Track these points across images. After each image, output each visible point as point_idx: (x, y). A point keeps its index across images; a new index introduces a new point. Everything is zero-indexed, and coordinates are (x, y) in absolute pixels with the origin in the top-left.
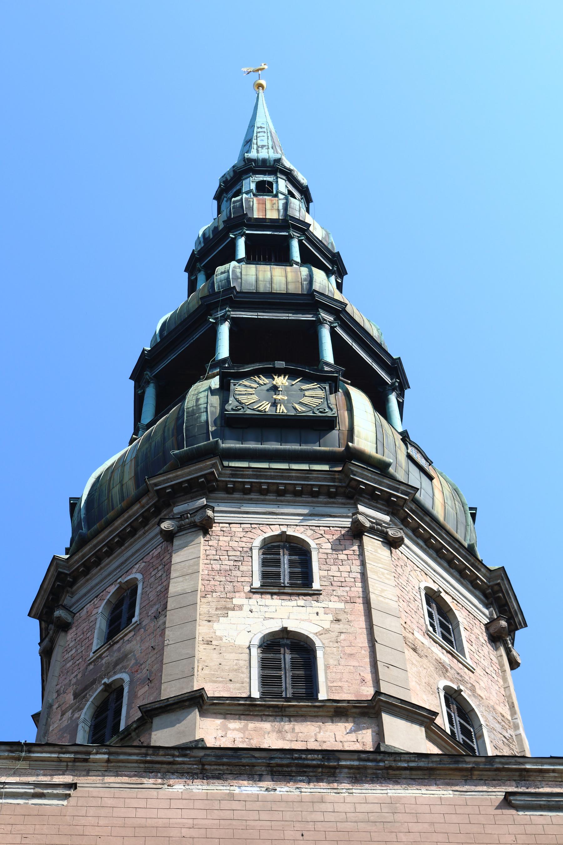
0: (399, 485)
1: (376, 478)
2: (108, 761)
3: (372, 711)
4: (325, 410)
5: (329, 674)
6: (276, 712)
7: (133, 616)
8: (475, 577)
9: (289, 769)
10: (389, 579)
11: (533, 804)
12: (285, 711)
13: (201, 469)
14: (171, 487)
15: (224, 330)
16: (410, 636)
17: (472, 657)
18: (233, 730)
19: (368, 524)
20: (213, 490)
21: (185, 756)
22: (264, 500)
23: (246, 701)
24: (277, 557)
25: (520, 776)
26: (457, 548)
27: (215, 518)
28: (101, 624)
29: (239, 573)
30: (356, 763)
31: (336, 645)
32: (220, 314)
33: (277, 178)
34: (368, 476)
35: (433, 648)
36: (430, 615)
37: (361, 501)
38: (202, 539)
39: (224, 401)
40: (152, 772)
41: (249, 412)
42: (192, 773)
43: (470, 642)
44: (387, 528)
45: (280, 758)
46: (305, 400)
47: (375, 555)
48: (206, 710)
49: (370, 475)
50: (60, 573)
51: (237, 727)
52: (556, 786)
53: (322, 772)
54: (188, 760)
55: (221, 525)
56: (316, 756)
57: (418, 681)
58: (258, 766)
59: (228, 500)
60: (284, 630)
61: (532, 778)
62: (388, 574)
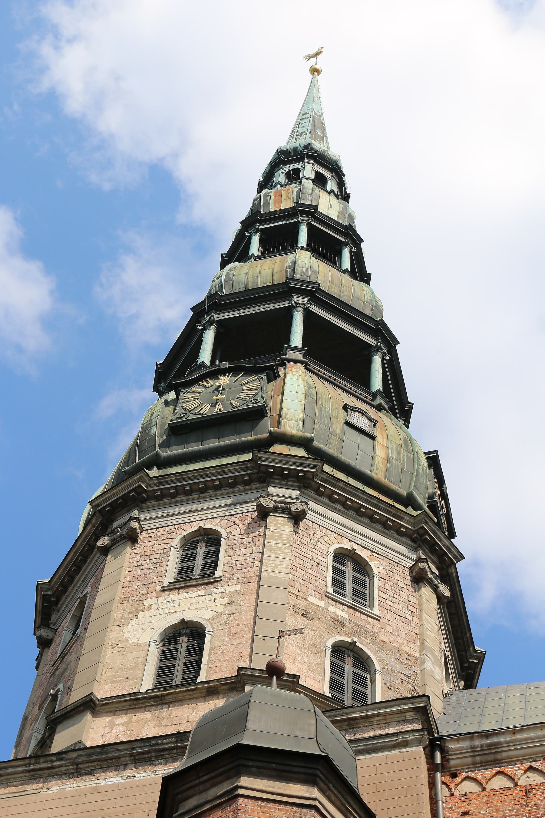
0: (306, 460)
1: (283, 459)
3: (239, 685)
4: (257, 400)
5: (212, 656)
6: (157, 701)
8: (399, 526)
9: (149, 755)
10: (285, 553)
12: (164, 699)
13: (131, 485)
14: (110, 505)
16: (303, 602)
17: (382, 604)
18: (119, 725)
20: (144, 501)
21: (61, 759)
23: (130, 696)
24: (195, 551)
25: (349, 725)
26: (375, 504)
29: (155, 575)
31: (225, 626)
32: (207, 319)
34: (275, 459)
35: (330, 609)
37: (272, 483)
38: (128, 550)
40: (36, 779)
41: (191, 417)
42: (69, 773)
43: (384, 590)
45: (140, 747)
46: (241, 395)
47: (277, 533)
48: (98, 711)
49: (277, 458)
51: (123, 722)
52: (381, 728)
53: (177, 753)
54: (64, 762)
55: (149, 531)
56: (170, 740)
57: (300, 645)
58: (123, 757)
59: (158, 506)
60: (183, 620)
61: (360, 725)
62: (285, 548)
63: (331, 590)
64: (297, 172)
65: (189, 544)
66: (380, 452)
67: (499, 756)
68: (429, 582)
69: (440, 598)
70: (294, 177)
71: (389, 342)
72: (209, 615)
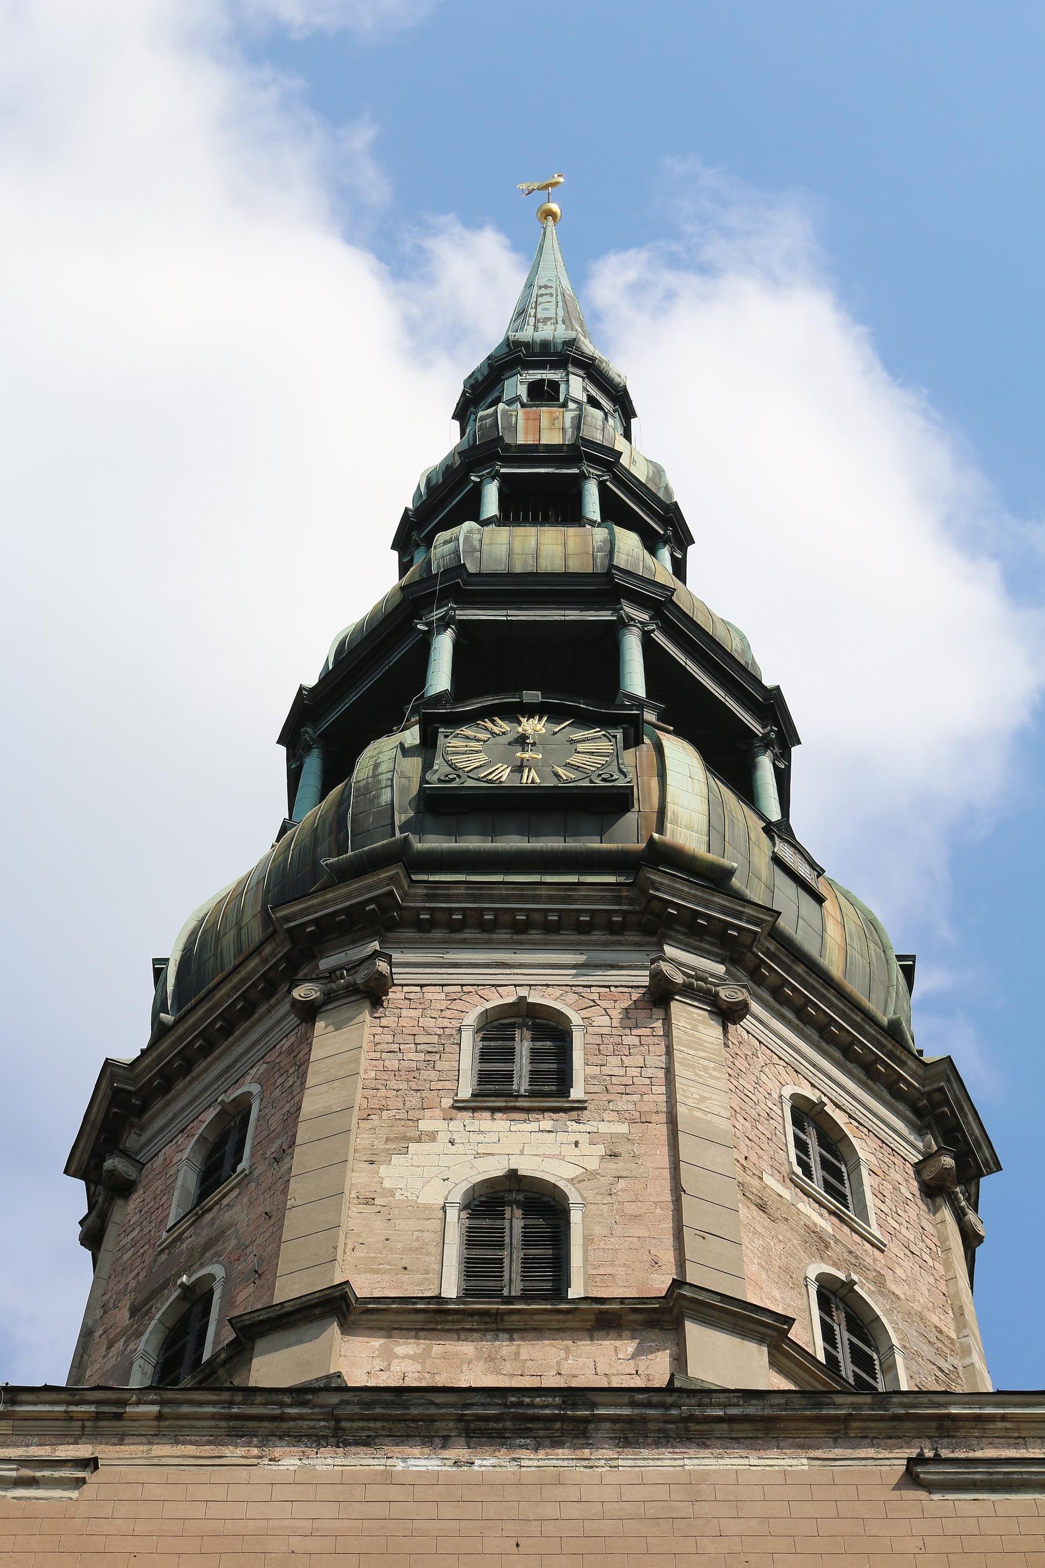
0: (744, 906)
1: (698, 893)
2: (160, 1417)
3: (667, 1317)
4: (612, 776)
5: (591, 1253)
6: (486, 1323)
7: (240, 1160)
8: (895, 1077)
9: (500, 1425)
11: (960, 1480)
12: (502, 1320)
13: (370, 888)
14: (316, 921)
15: (444, 646)
16: (755, 1182)
17: (882, 1222)
18: (403, 1358)
19: (679, 979)
20: (393, 926)
21: (303, 1404)
22: (489, 942)
23: (429, 1303)
24: (509, 1043)
25: (939, 1428)
26: (858, 1023)
27: (394, 976)
28: (187, 1180)
29: (433, 1075)
30: (626, 1411)
31: (608, 1199)
32: (437, 614)
33: (567, 375)
34: (682, 891)
35: (801, 1206)
36: (801, 1146)
37: (671, 938)
38: (366, 1015)
39: (427, 766)
40: (243, 1436)
41: (470, 783)
42: (316, 1436)
43: (881, 1196)
44: (716, 985)
45: (483, 1405)
46: (576, 759)
47: (693, 1036)
48: (354, 1322)
49: (687, 889)
50: (117, 1090)
51: (412, 1353)
52: (1009, 1446)
53: (562, 1429)
54: (309, 1411)
55: (406, 989)
56: (550, 1399)
57: (764, 1264)
58: (441, 1420)
59: (421, 943)
60: (513, 1174)
61: (963, 1432)
62: (714, 1069)
72: (572, 1172)
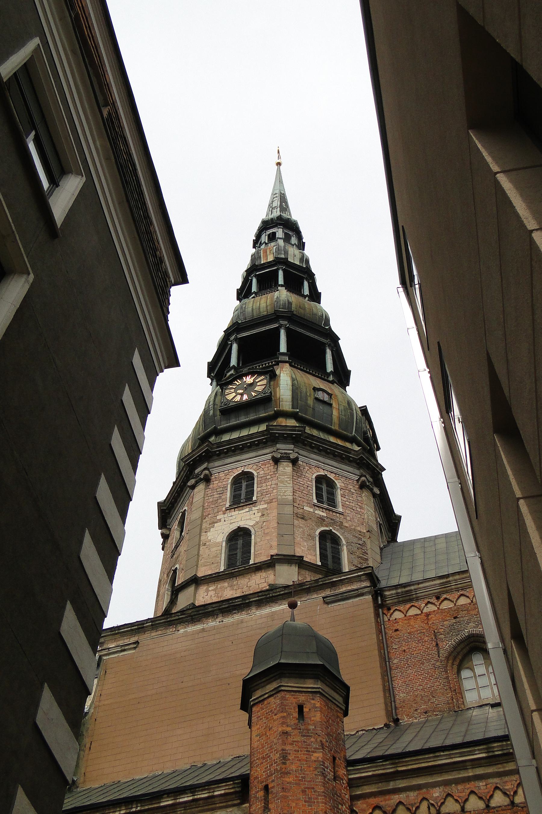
2: (152, 625)
10: (289, 483)
16: (301, 511)
20: (211, 457)
21: (184, 614)
22: (235, 454)
30: (257, 598)
35: (316, 512)
63: (315, 501)
64: (274, 234)
65: (236, 481)
66: (335, 413)
67: (411, 597)
68: (368, 487)
69: (374, 495)
70: (272, 237)
71: (334, 339)
72: (252, 523)
